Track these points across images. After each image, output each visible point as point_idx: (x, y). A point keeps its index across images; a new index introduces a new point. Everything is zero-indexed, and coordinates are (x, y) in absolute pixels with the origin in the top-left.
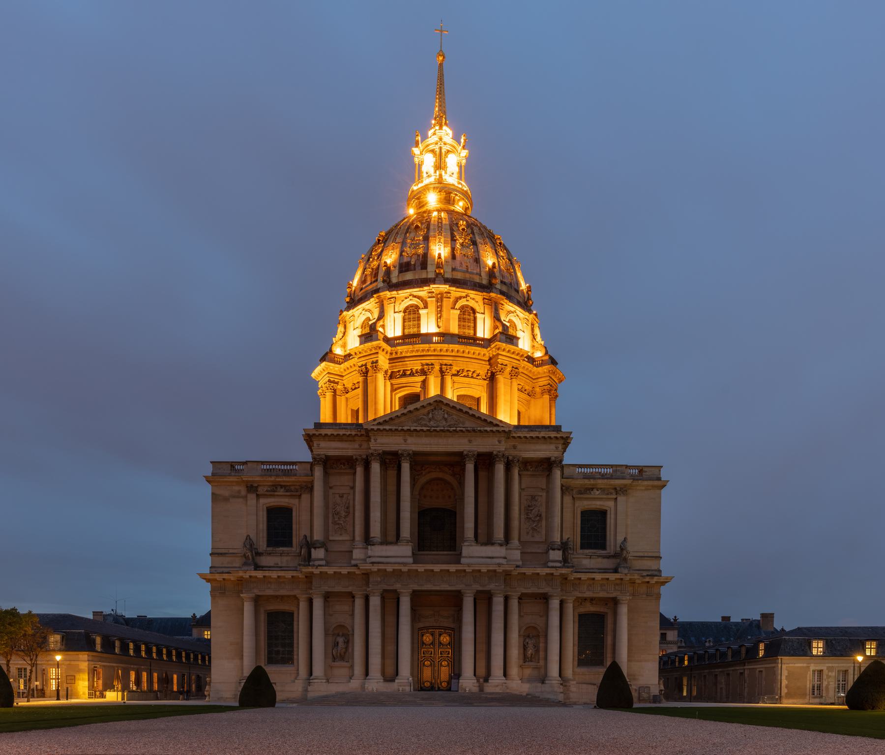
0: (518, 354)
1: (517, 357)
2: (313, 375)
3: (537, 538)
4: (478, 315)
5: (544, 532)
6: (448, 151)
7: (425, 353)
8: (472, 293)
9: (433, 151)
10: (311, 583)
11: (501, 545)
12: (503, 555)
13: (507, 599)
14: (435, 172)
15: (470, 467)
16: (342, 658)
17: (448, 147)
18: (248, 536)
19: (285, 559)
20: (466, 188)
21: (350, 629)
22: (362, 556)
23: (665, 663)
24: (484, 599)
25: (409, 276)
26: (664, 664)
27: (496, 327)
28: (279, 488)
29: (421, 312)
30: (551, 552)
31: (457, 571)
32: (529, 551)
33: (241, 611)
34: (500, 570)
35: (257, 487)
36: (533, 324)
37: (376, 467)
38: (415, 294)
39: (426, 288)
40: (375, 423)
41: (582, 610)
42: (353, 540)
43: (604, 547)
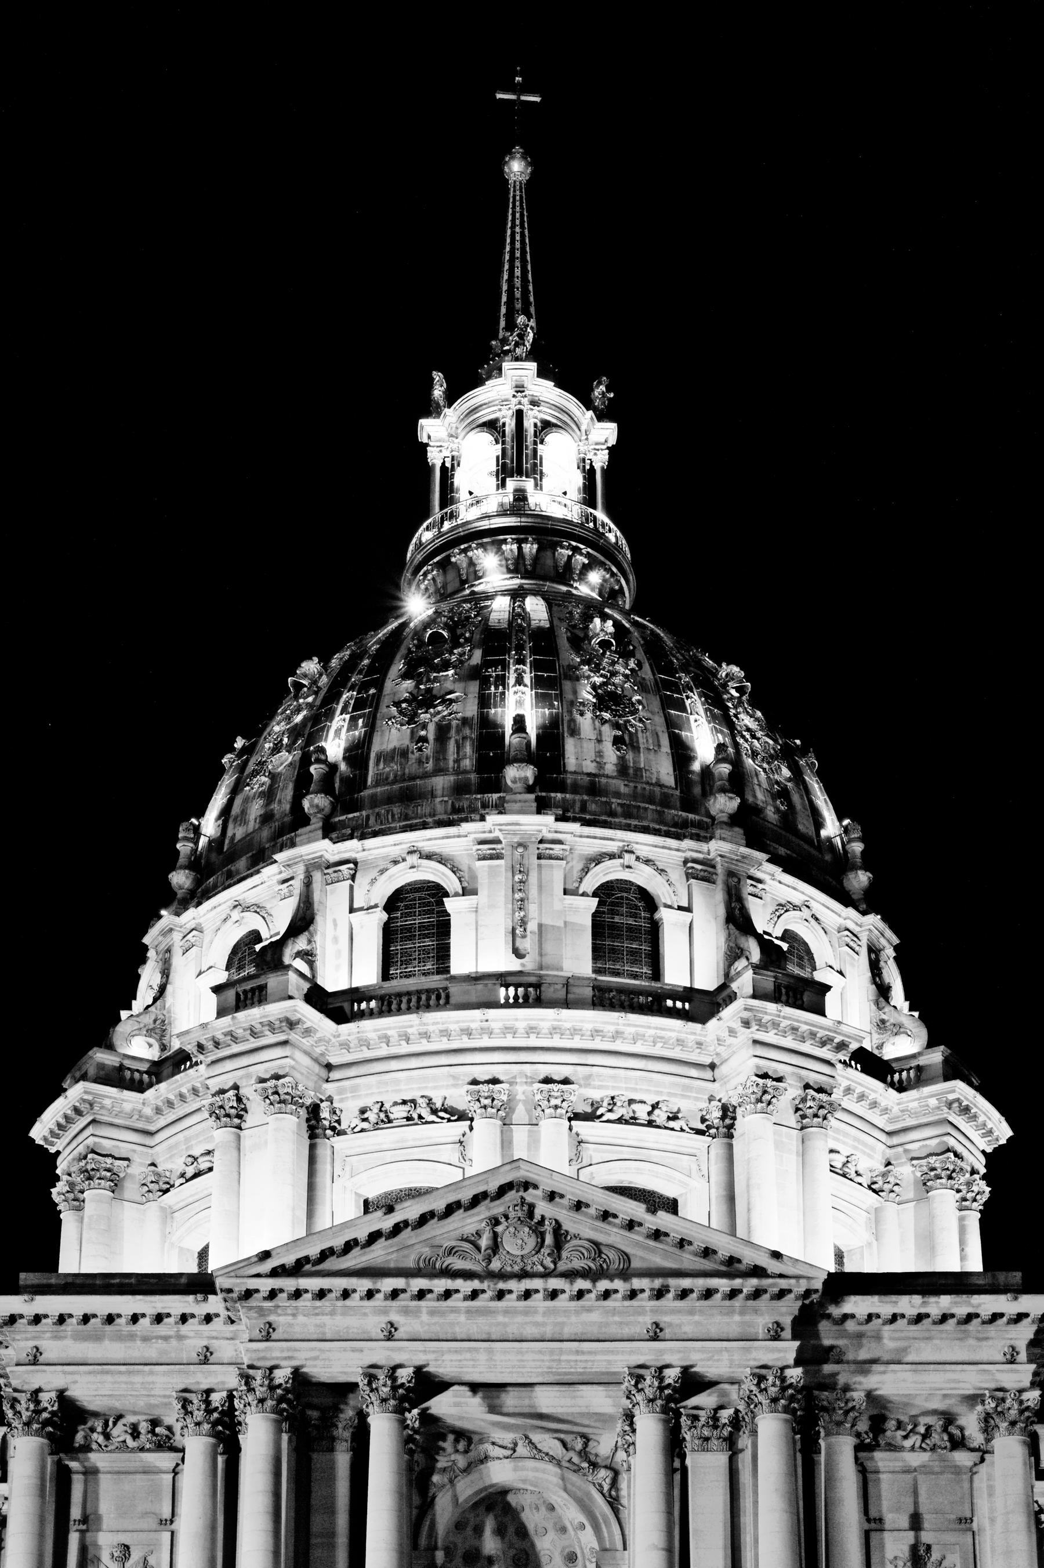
0: (823, 1044)
1: (825, 1053)
2: (38, 1132)
4: (665, 915)
6: (547, 425)
7: (466, 1043)
8: (644, 843)
9: (492, 426)
14: (503, 484)
17: (545, 413)
20: (614, 535)
27: (734, 953)
29: (450, 904)
36: (874, 951)
38: (428, 847)
39: (466, 827)
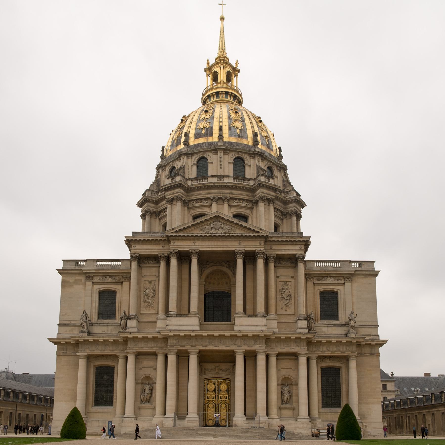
3: (289, 312)
5: (293, 307)
10: (127, 344)
11: (263, 316)
12: (263, 324)
13: (268, 357)
15: (240, 262)
16: (148, 401)
18: (84, 312)
19: (110, 328)
21: (154, 379)
22: (164, 326)
23: (387, 406)
24: (250, 358)
25: (201, 140)
26: (386, 407)
28: (108, 277)
30: (299, 321)
31: (231, 336)
32: (283, 321)
33: (77, 365)
34: (262, 335)
35: (92, 277)
37: (174, 262)
40: (174, 231)
41: (324, 365)
42: (157, 314)
43: (336, 318)
